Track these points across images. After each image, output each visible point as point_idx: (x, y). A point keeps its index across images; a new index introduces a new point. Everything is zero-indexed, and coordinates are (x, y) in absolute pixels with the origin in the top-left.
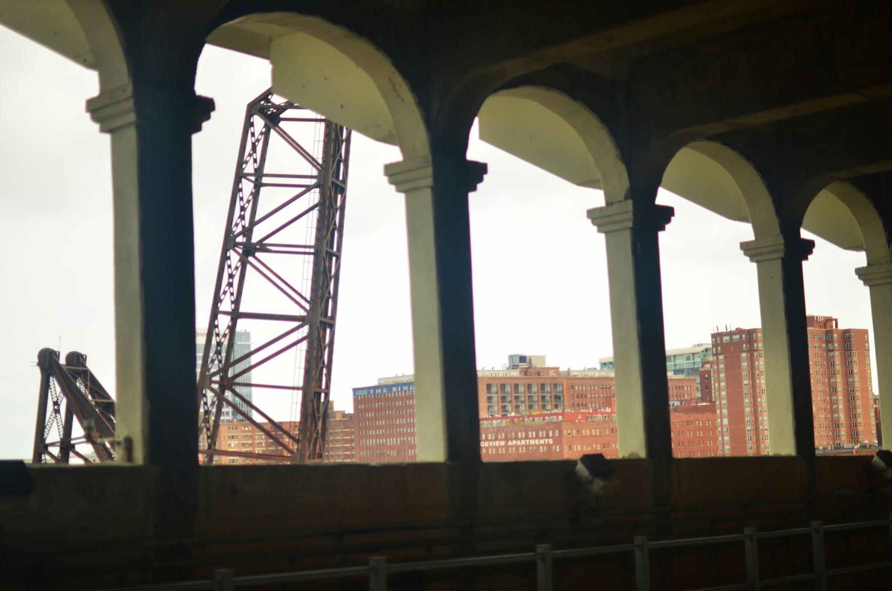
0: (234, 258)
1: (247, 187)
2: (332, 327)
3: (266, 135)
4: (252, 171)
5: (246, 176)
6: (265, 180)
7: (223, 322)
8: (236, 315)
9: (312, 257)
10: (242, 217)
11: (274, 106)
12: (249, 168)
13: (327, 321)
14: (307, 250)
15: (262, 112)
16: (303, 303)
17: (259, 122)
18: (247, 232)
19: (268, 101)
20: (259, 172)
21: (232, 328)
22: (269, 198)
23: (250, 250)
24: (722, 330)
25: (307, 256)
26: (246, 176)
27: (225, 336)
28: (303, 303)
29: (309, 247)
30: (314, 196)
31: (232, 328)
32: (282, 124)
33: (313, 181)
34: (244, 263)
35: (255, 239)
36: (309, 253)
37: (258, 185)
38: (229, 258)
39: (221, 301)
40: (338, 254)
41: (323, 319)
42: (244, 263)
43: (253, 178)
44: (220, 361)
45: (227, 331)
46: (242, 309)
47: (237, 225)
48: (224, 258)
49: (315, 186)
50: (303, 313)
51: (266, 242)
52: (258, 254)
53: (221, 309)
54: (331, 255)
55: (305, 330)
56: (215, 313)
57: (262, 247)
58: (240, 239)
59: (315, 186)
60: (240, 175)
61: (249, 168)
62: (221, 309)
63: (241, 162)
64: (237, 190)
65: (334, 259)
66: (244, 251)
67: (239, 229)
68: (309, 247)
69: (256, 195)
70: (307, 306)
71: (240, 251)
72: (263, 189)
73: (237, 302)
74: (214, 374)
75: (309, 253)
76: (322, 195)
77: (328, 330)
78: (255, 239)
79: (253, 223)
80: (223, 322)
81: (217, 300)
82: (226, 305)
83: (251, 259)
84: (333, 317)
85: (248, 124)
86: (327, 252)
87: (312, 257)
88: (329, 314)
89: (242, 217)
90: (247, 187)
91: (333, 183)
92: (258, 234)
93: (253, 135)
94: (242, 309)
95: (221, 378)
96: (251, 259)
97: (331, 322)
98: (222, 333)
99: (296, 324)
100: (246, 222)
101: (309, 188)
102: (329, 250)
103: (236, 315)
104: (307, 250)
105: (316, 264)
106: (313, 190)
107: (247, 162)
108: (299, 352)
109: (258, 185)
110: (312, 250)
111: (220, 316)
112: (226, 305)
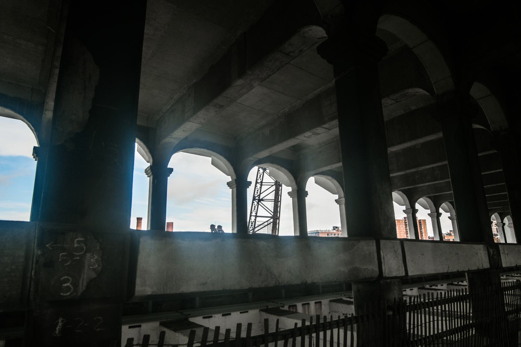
0: (255, 203)
1: (259, 186)
2: (279, 219)
3: (263, 173)
4: (260, 182)
5: (258, 183)
6: (263, 184)
8: (256, 216)
9: (273, 202)
10: (257, 193)
12: (259, 181)
13: (278, 218)
14: (272, 200)
20: (262, 182)
21: (255, 220)
22: (264, 188)
23: (260, 200)
26: (258, 183)
27: (253, 221)
29: (273, 200)
31: (255, 220)
35: (261, 198)
36: (273, 201)
37: (261, 185)
38: (254, 203)
39: (252, 213)
41: (276, 217)
43: (260, 183)
44: (252, 228)
45: (254, 220)
46: (258, 215)
47: (256, 195)
48: (253, 202)
50: (271, 216)
51: (263, 199)
52: (261, 202)
53: (252, 215)
54: (278, 202)
55: (272, 220)
56: (251, 216)
57: (262, 200)
58: (257, 198)
61: (259, 181)
62: (252, 215)
65: (279, 202)
66: (258, 201)
67: (257, 195)
68: (273, 200)
69: (261, 188)
70: (272, 214)
71: (257, 201)
73: (256, 213)
75: (273, 201)
77: (278, 220)
78: (261, 198)
79: (260, 193)
81: (251, 213)
82: (254, 214)
83: (260, 203)
87: (273, 202)
88: (278, 216)
89: (257, 193)
90: (259, 186)
94: (258, 215)
95: (253, 232)
96: (260, 203)
97: (279, 218)
98: (252, 221)
99: (270, 218)
100: (259, 194)
102: (278, 200)
103: (256, 216)
104: (272, 200)
107: (258, 180)
109: (261, 185)
110: (274, 200)
111: (252, 217)
112: (254, 214)
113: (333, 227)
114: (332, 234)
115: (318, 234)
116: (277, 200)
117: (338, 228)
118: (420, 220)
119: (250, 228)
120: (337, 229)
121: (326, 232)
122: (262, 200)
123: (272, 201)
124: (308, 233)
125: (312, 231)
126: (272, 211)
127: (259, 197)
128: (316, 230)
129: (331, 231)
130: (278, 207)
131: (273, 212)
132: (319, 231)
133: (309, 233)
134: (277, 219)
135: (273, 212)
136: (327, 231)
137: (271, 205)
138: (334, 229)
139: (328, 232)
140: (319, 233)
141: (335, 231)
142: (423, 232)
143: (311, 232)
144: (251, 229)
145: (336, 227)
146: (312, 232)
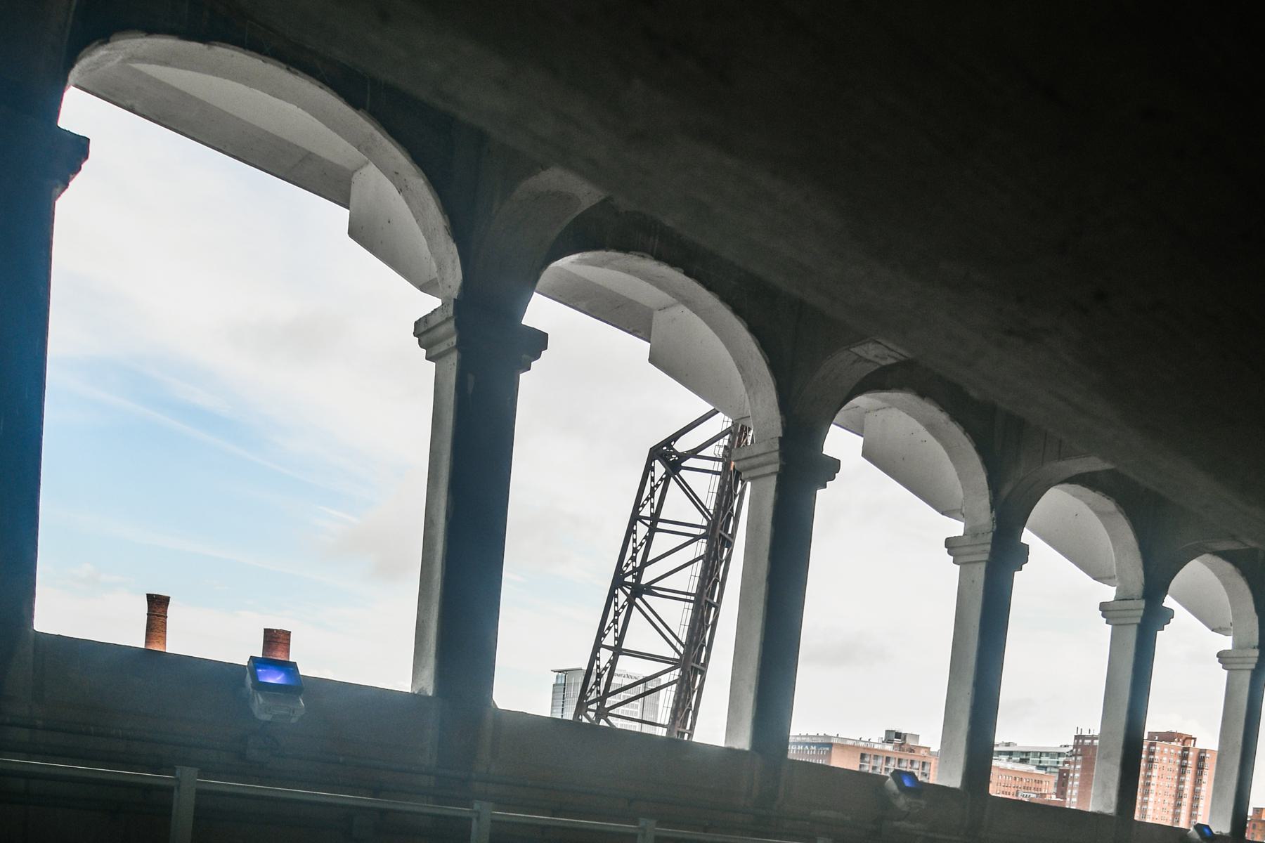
0: (622, 598)
1: (642, 530)
2: (703, 673)
3: (666, 481)
5: (641, 519)
6: (660, 525)
7: (606, 656)
8: (618, 651)
9: (691, 604)
10: (633, 559)
11: (676, 452)
12: (646, 512)
13: (699, 667)
14: (688, 597)
15: (664, 458)
16: (678, 646)
17: (660, 469)
18: (639, 571)
19: (671, 447)
20: (655, 517)
21: (613, 663)
22: (662, 542)
23: (639, 590)
24: (1085, 733)
25: (687, 603)
26: (641, 519)
27: (605, 669)
28: (678, 646)
30: (700, 548)
31: (613, 663)
32: (682, 473)
33: (703, 531)
34: (631, 603)
35: (643, 582)
36: (690, 601)
37: (653, 530)
38: (617, 596)
39: (605, 636)
40: (717, 605)
41: (695, 665)
42: (631, 603)
43: (648, 522)
44: (598, 692)
47: (627, 565)
49: (702, 536)
50: (677, 657)
52: (644, 596)
54: (711, 605)
55: (676, 673)
57: (649, 589)
58: (629, 579)
59: (702, 536)
60: (635, 517)
61: (646, 512)
63: (638, 505)
64: (631, 531)
65: (713, 609)
67: (630, 568)
69: (649, 539)
70: (682, 650)
71: (628, 591)
72: (657, 534)
73: (620, 639)
74: (592, 702)
75: (690, 601)
76: (709, 546)
77: (699, 676)
78: (643, 582)
79: (645, 563)
80: (606, 656)
82: (609, 640)
83: (638, 600)
84: (705, 665)
85: (649, 468)
86: (706, 601)
87: (691, 604)
88: (702, 661)
89: (633, 559)
90: (642, 530)
91: (720, 535)
92: (648, 575)
93: (653, 479)
94: (626, 645)
96: (638, 600)
97: (703, 668)
98: (602, 666)
101: (696, 538)
103: (618, 651)
104: (688, 597)
105: (695, 611)
106: (701, 540)
107: (643, 506)
108: (668, 692)
109: (653, 530)
110: (693, 598)
112: (609, 640)
113: (887, 731)
114: (876, 757)
115: (828, 749)
116: (705, 598)
117: (905, 739)
118: (1204, 751)
119: (591, 690)
120: (898, 741)
121: (858, 747)
122: (649, 589)
123: (685, 600)
124: (791, 740)
125: (807, 736)
126: (680, 638)
127: (638, 578)
128: (821, 734)
129: (876, 747)
130: (707, 628)
131: (684, 641)
132: (833, 741)
133: (794, 743)
134: (696, 671)
135: (684, 641)
136: (862, 744)
137: (678, 615)
138: (889, 741)
139: (864, 748)
140: (830, 745)
141: (889, 747)
142: (1203, 794)
143: (804, 739)
144: (593, 696)
145: (898, 735)
146: (808, 740)
